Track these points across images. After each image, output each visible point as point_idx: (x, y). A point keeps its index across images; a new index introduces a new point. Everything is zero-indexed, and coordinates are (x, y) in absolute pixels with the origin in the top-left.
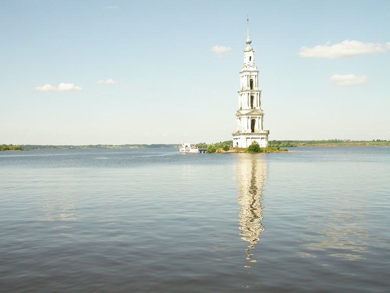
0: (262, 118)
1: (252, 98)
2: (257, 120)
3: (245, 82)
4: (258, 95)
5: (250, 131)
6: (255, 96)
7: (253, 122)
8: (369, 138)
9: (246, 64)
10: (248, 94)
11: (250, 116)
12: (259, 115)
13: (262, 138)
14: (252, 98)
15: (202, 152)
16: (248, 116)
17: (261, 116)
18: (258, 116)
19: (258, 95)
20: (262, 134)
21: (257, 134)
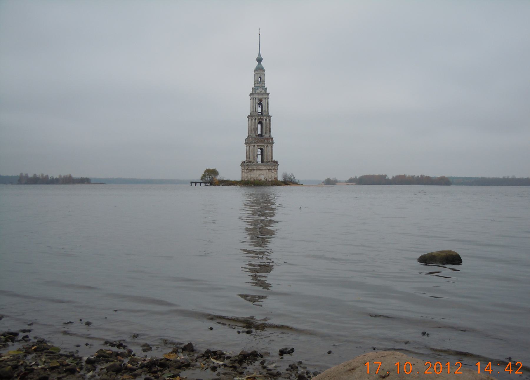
10: (255, 119)
11: (256, 145)
12: (267, 143)
16: (253, 145)
17: (268, 145)
18: (266, 145)
20: (269, 165)
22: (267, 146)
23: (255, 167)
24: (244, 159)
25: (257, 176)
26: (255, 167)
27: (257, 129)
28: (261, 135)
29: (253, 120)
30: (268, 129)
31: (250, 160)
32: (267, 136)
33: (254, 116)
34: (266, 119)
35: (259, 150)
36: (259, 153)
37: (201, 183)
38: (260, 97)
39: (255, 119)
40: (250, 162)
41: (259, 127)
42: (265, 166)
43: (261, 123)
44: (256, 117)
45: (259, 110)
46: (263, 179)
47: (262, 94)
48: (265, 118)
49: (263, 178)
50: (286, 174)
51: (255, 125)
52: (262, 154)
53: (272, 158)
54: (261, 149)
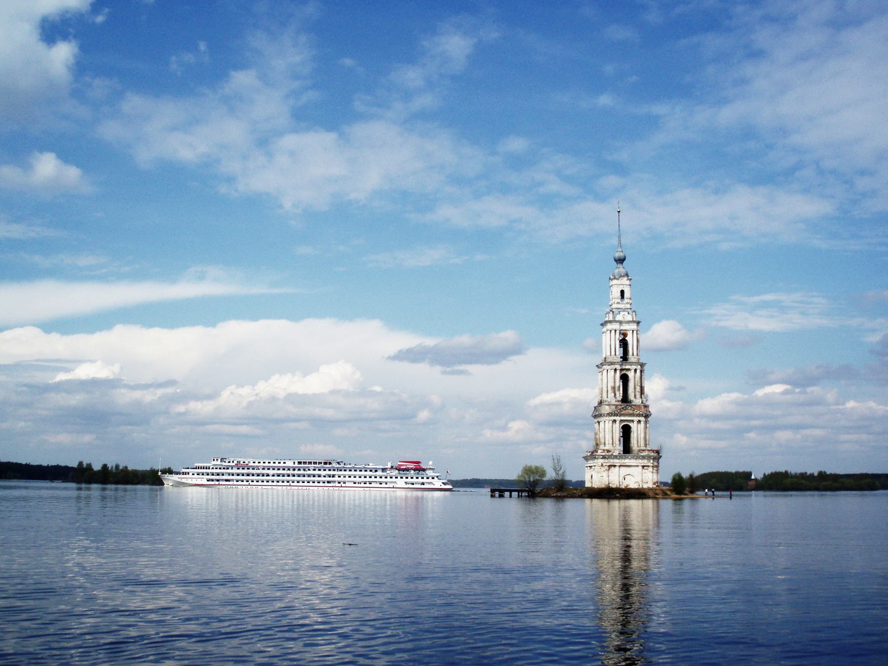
0: (646, 422)
1: (625, 379)
2: (634, 426)
3: (609, 345)
4: (638, 371)
5: (618, 448)
6: (631, 374)
7: (626, 431)
8: (813, 469)
9: (614, 306)
10: (615, 370)
11: (618, 418)
13: (643, 467)
14: (625, 379)
15: (497, 494)
17: (642, 419)
18: (636, 419)
19: (638, 371)
20: (643, 457)
21: (638, 458)
22: (639, 422)
25: (621, 478)
29: (612, 373)
30: (638, 389)
31: (607, 448)
32: (638, 401)
34: (636, 370)
38: (625, 327)
39: (615, 370)
40: (608, 451)
42: (633, 458)
48: (634, 367)
50: (679, 475)
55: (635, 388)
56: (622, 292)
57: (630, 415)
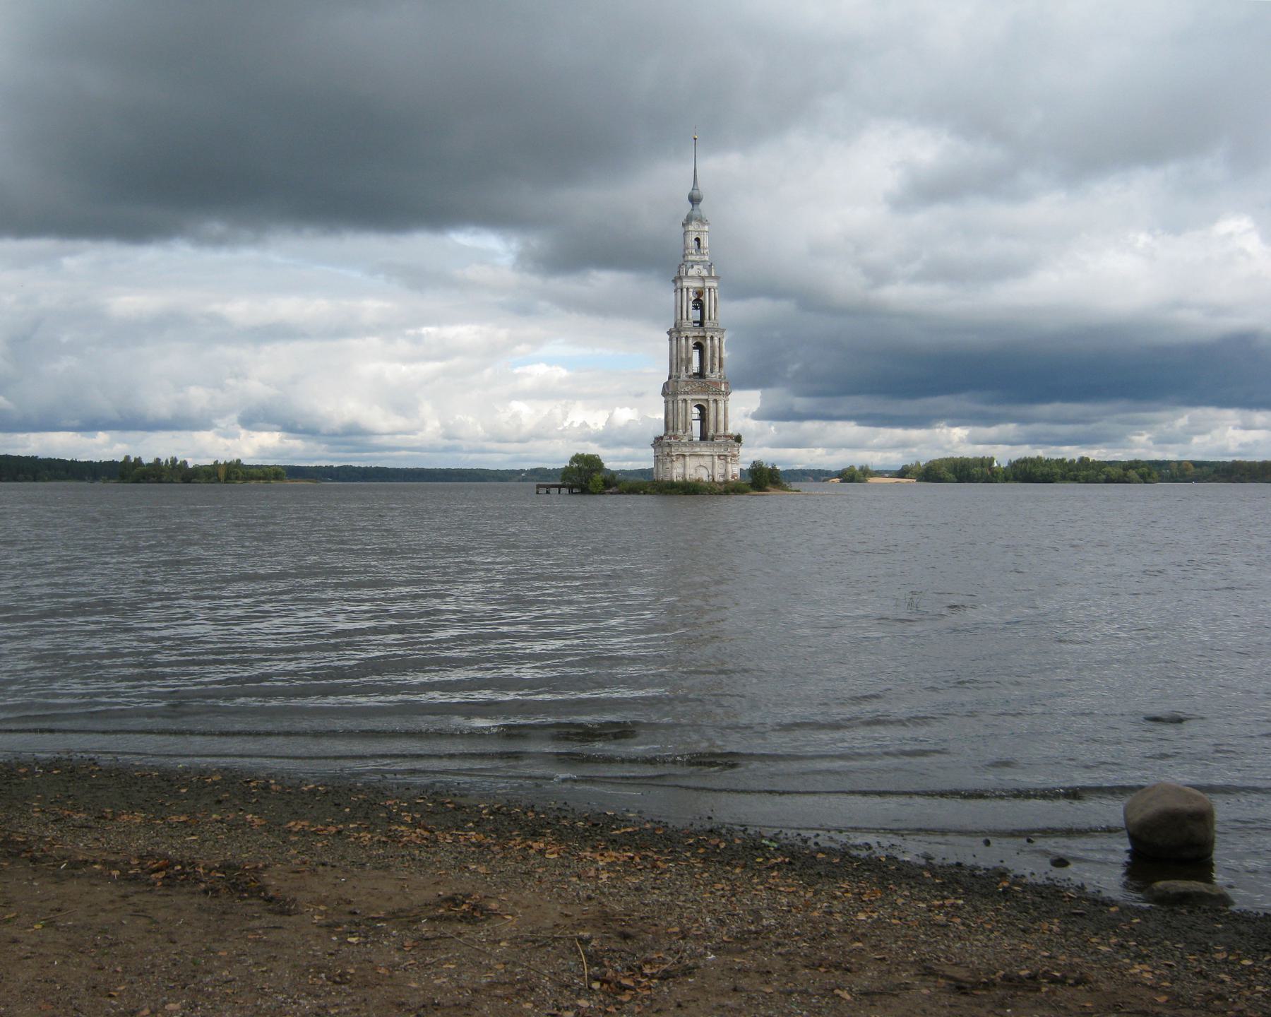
10: (687, 338)
11: (687, 397)
17: (717, 397)
18: (711, 398)
20: (719, 445)
22: (716, 401)
23: (686, 450)
24: (662, 432)
26: (686, 450)
27: (689, 361)
28: (701, 374)
29: (683, 340)
33: (685, 330)
34: (712, 338)
35: (696, 411)
36: (696, 416)
37: (559, 487)
38: (698, 284)
39: (687, 338)
41: (695, 355)
43: (699, 346)
44: (689, 333)
45: (696, 315)
46: (705, 478)
47: (703, 279)
49: (704, 475)
51: (687, 352)
52: (703, 418)
53: (725, 429)
54: (700, 407)
55: (712, 360)
56: (697, 240)
57: (703, 392)
